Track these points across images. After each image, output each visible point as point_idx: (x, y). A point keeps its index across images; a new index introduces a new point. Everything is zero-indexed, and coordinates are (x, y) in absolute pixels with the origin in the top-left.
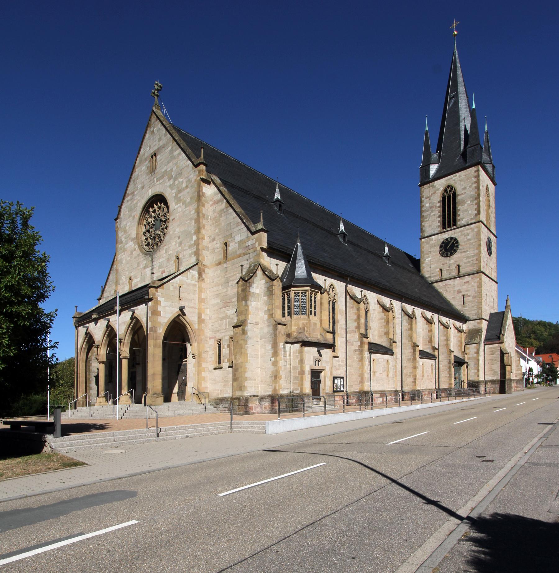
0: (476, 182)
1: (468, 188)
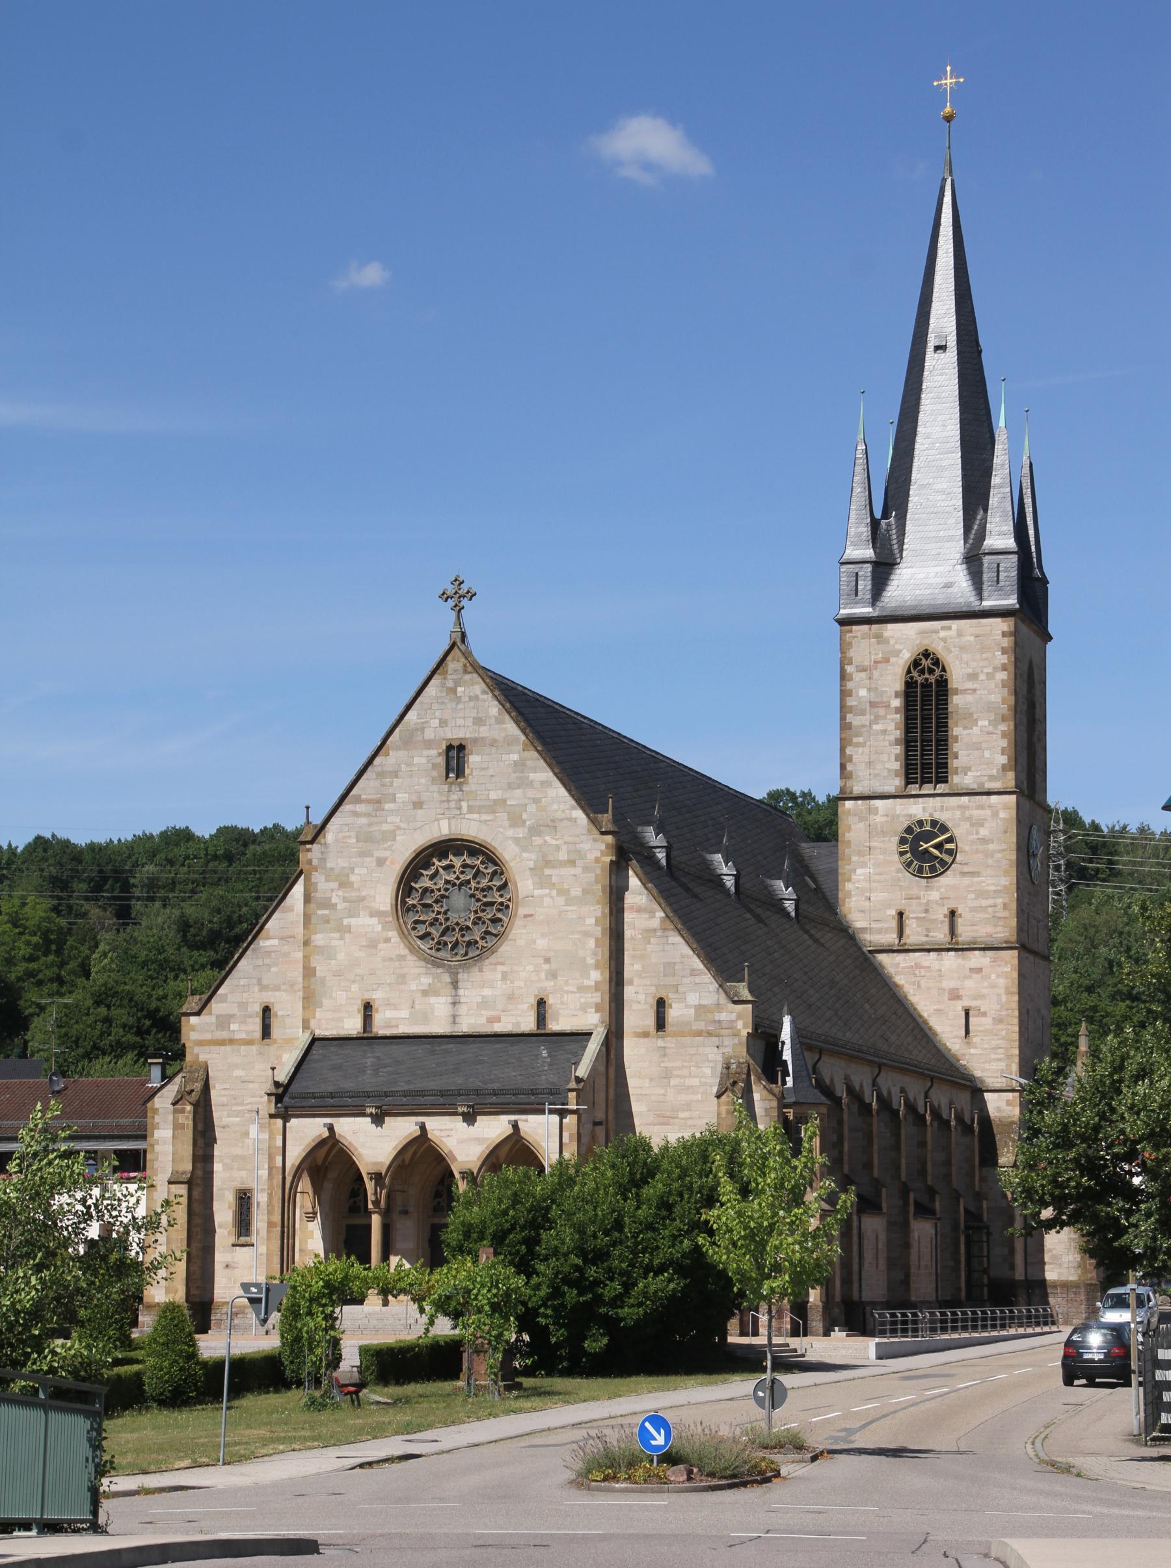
1: (982, 677)
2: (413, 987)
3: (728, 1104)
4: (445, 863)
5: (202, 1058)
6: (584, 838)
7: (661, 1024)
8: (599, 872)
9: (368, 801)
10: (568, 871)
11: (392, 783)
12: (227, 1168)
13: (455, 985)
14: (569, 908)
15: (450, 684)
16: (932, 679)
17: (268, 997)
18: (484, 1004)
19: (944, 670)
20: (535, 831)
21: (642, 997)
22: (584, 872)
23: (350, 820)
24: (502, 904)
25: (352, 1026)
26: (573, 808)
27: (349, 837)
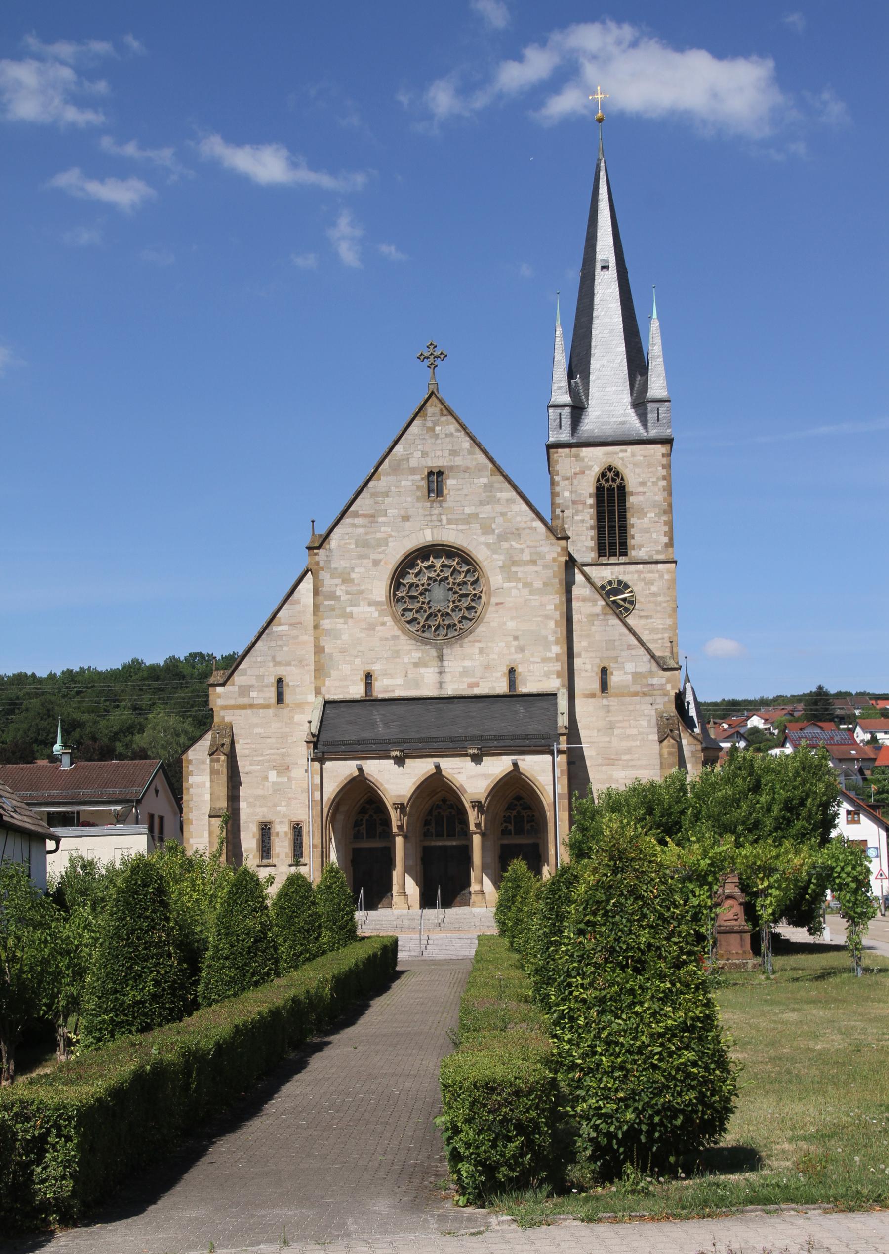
0: (664, 478)
1: (649, 484)
2: (406, 660)
3: (669, 747)
4: (426, 564)
5: (227, 719)
6: (543, 543)
7: (604, 686)
8: (556, 569)
9: (365, 516)
10: (532, 568)
11: (384, 501)
12: (250, 805)
13: (441, 658)
14: (532, 597)
15: (429, 424)
16: (615, 485)
17: (281, 671)
18: (465, 672)
19: (622, 479)
20: (502, 537)
21: (588, 667)
22: (544, 569)
23: (350, 530)
24: (475, 595)
25: (357, 691)
26: (533, 520)
27: (350, 544)
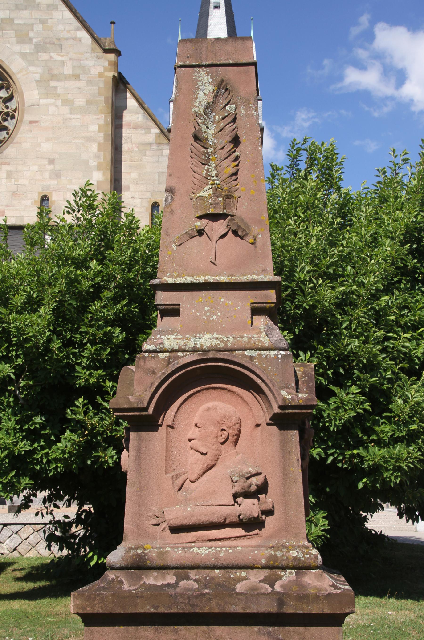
6: (88, 55)
8: (102, 85)
10: (73, 84)
14: (73, 116)
20: (41, 47)
26: (77, 29)
